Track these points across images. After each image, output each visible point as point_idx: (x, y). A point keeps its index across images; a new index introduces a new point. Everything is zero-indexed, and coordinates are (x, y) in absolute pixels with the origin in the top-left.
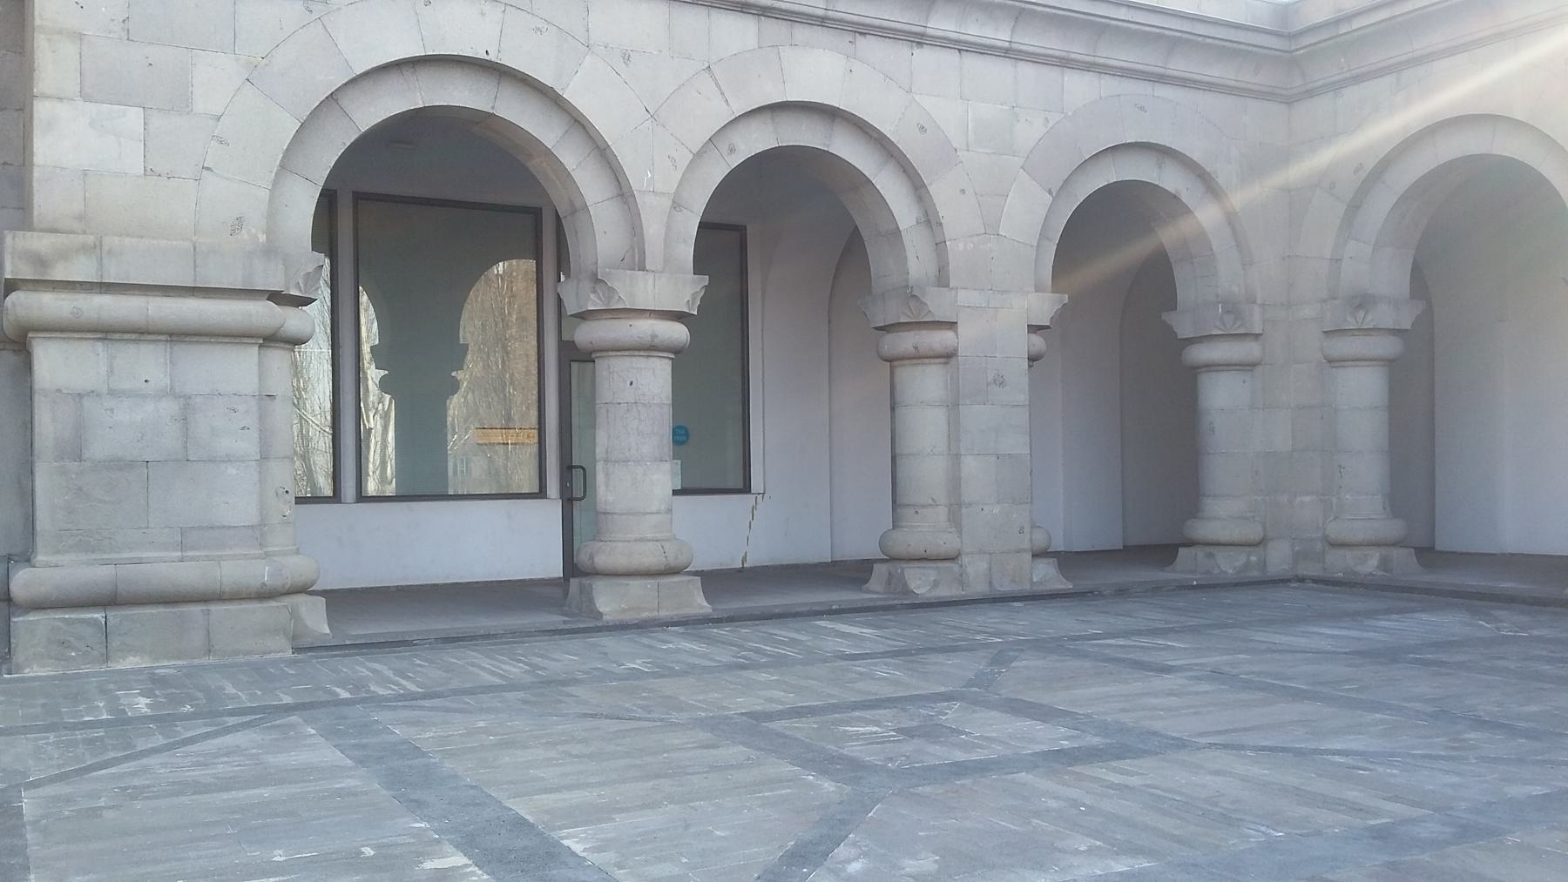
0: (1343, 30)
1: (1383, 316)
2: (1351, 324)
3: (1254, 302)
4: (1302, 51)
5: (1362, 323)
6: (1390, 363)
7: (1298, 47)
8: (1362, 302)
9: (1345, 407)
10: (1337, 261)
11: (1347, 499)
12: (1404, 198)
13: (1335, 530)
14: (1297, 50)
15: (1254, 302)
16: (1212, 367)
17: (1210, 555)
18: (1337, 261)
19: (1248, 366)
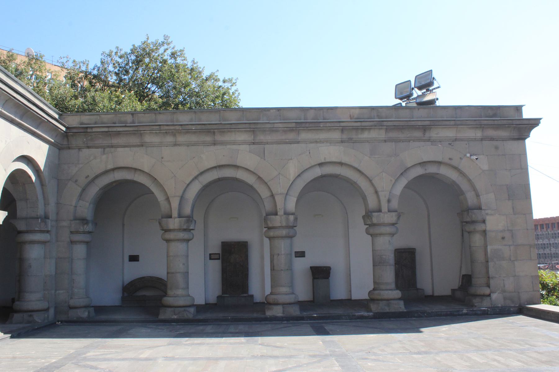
0: (89, 130)
1: (89, 228)
2: (81, 229)
3: (49, 219)
4: (71, 133)
5: (86, 229)
6: (87, 243)
7: (70, 132)
8: (84, 221)
9: (76, 258)
10: (76, 207)
11: (76, 291)
12: (100, 189)
13: (72, 302)
14: (69, 133)
15: (49, 219)
16: (32, 242)
17: (31, 316)
18: (76, 207)
19: (44, 243)
